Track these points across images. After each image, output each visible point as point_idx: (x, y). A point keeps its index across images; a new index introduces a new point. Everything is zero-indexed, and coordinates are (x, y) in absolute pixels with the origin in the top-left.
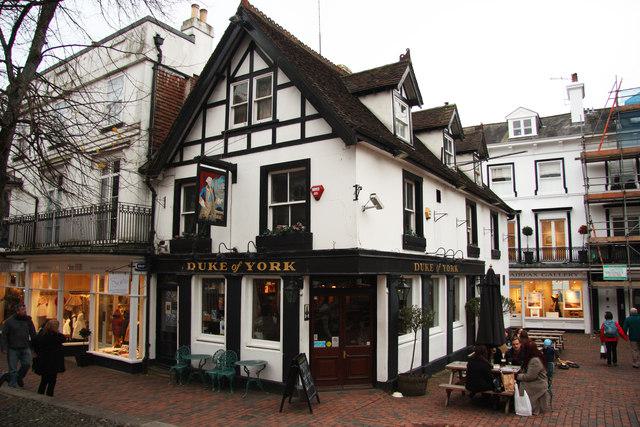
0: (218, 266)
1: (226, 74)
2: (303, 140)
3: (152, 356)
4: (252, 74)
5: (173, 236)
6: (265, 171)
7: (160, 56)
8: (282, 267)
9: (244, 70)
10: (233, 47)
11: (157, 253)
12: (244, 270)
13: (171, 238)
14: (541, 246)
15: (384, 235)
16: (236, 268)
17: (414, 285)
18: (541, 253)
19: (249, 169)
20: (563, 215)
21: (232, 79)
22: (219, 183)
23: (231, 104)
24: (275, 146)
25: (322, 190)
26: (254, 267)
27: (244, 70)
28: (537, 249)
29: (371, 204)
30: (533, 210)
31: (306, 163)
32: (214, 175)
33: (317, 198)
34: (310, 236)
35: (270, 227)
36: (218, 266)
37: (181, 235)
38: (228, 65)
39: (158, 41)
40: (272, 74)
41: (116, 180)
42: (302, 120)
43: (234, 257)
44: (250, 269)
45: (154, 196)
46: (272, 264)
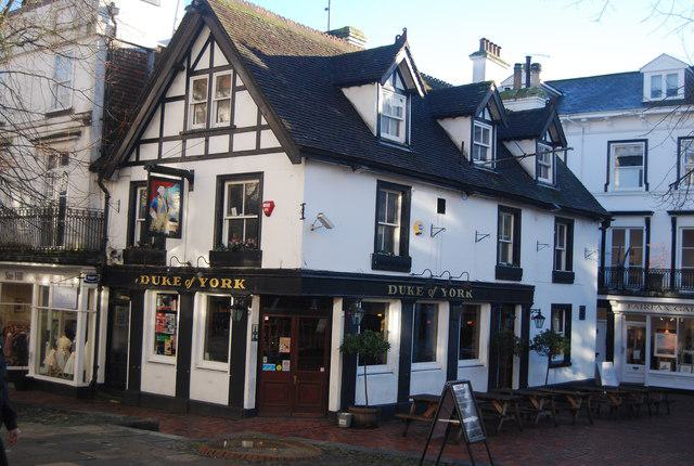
0: (172, 281)
1: (185, 65)
2: (258, 151)
3: (101, 379)
4: (211, 70)
5: (127, 245)
6: (222, 179)
8: (233, 284)
9: (204, 64)
10: (145, 120)
11: (109, 263)
12: (197, 287)
14: (679, 266)
15: (352, 255)
16: (189, 284)
18: (679, 277)
19: (207, 173)
20: (639, 222)
21: (191, 73)
23: (191, 101)
24: (231, 154)
25: (272, 206)
26: (207, 284)
27: (204, 64)
28: (673, 271)
29: (319, 223)
31: (259, 175)
33: (268, 214)
34: (260, 253)
36: (172, 281)
37: (136, 244)
38: (188, 55)
40: (231, 72)
42: (258, 129)
43: (189, 272)
44: (203, 285)
45: (108, 198)
46: (224, 281)
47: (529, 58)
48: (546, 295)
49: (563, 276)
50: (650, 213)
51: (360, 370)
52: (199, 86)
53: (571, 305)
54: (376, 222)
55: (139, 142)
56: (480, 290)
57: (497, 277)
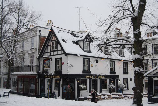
2: (61, 54)
4: (54, 40)
6: (56, 59)
7: (40, 34)
9: (53, 39)
13: (42, 71)
19: (54, 58)
21: (51, 41)
22: (49, 62)
23: (51, 46)
24: (57, 55)
25: (63, 63)
27: (53, 39)
29: (71, 66)
30: (152, 60)
31: (61, 58)
32: (47, 60)
33: (63, 65)
35: (57, 69)
39: (40, 31)
41: (33, 59)
43: (51, 76)
45: (40, 63)
48: (122, 77)
49: (126, 72)
50: (148, 60)
51: (81, 91)
52: (53, 44)
54: (83, 65)
55: (44, 53)
56: (106, 76)
57: (110, 74)
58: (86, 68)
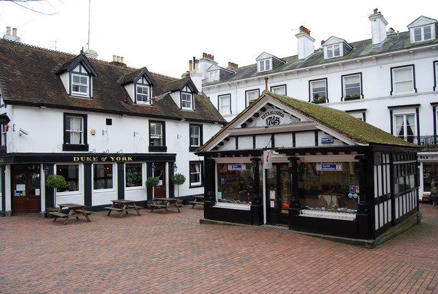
15: (54, 145)
17: (80, 166)
47: (194, 58)
53: (190, 162)
56: (138, 157)
58: (74, 140)
